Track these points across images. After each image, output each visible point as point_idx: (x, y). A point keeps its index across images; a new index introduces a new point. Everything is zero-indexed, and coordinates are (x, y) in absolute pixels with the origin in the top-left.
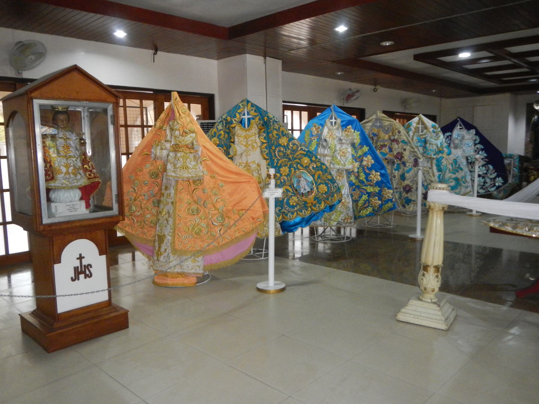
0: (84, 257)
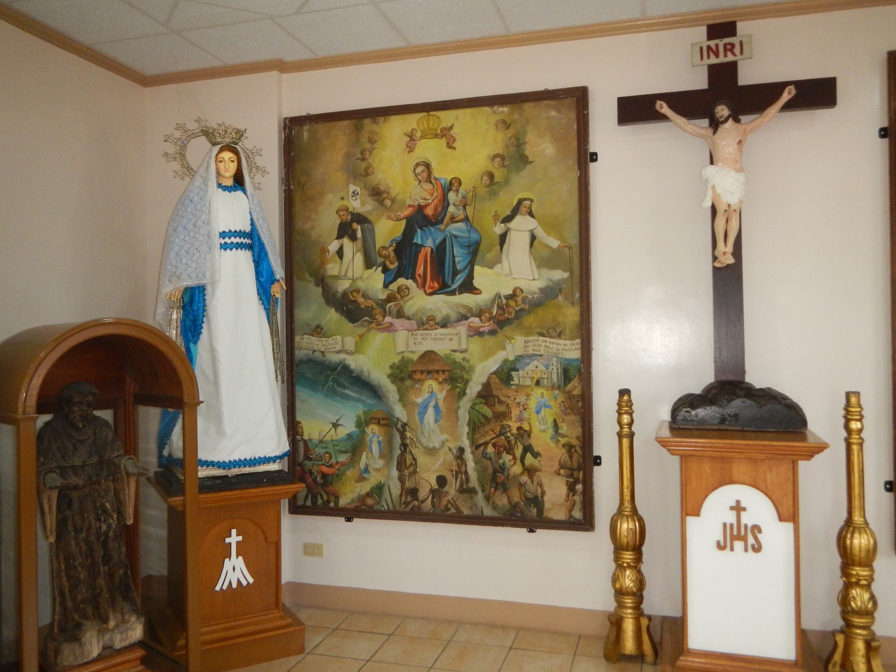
0: (744, 509)
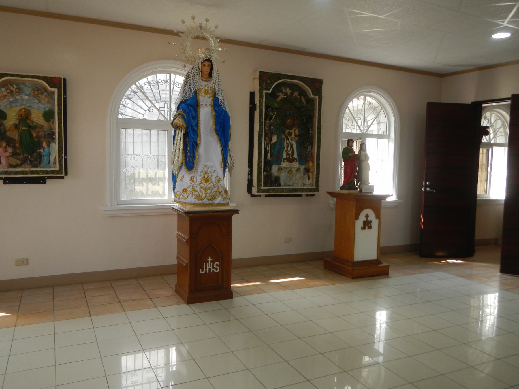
0: (369, 216)
